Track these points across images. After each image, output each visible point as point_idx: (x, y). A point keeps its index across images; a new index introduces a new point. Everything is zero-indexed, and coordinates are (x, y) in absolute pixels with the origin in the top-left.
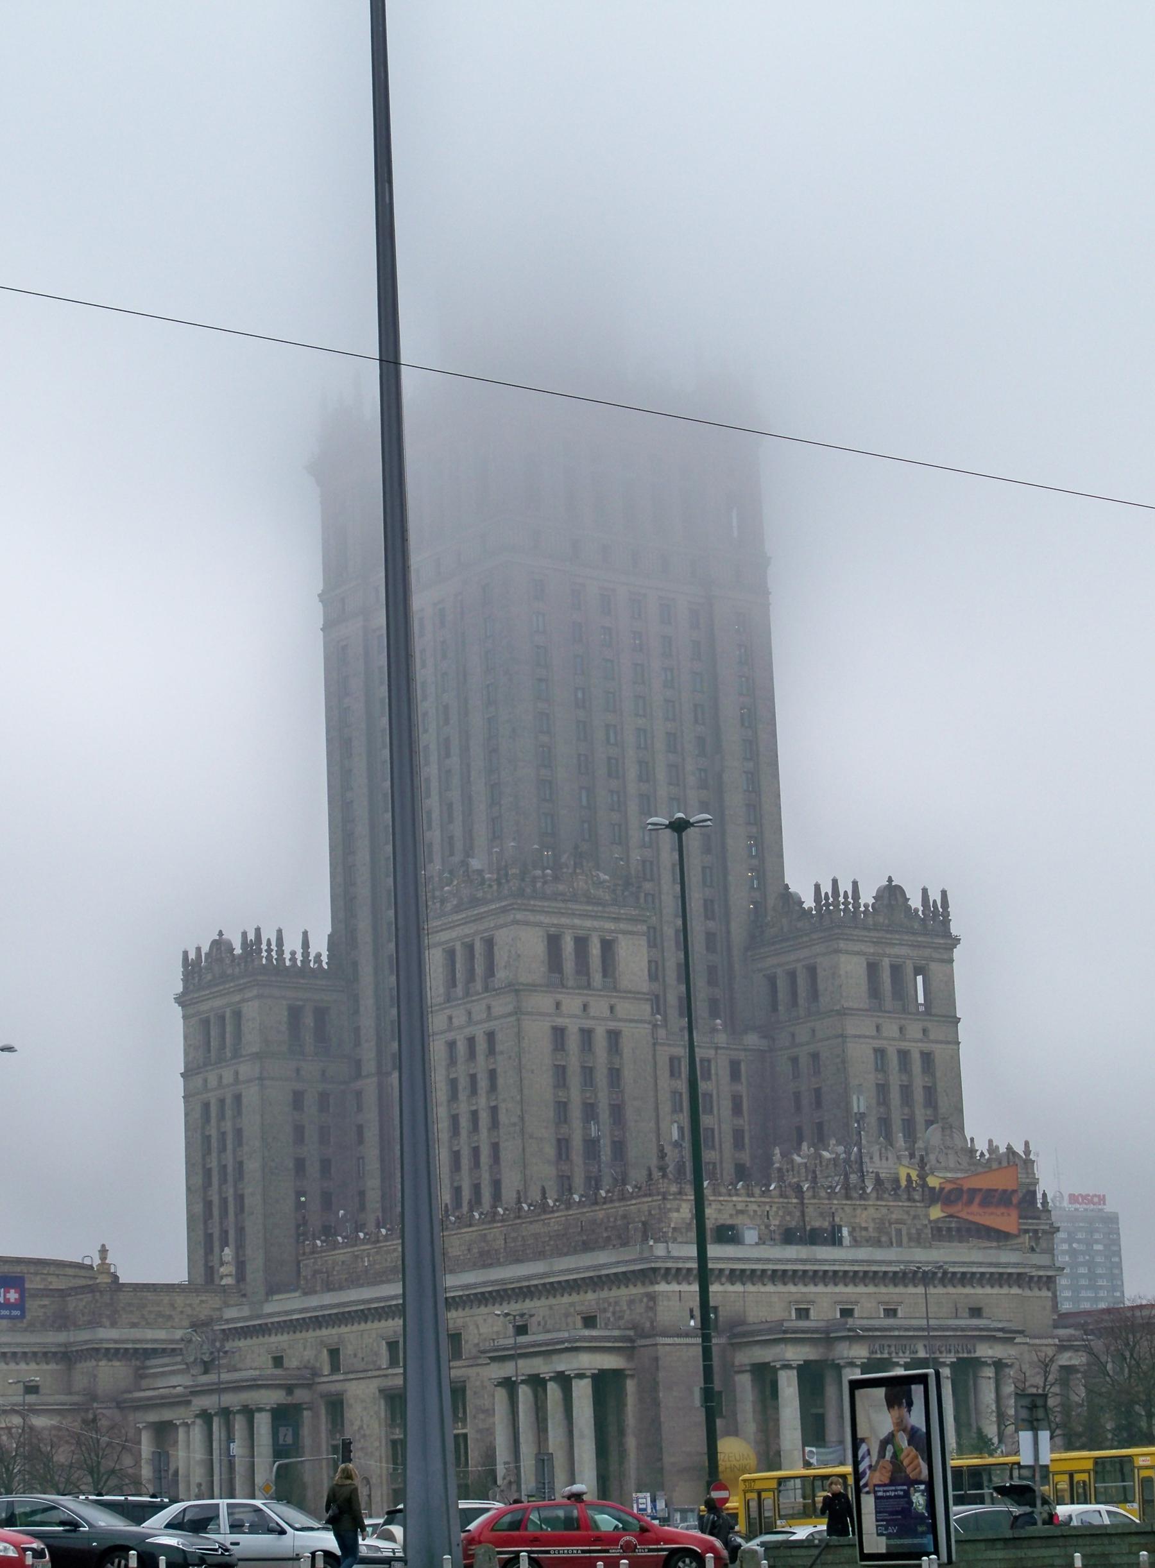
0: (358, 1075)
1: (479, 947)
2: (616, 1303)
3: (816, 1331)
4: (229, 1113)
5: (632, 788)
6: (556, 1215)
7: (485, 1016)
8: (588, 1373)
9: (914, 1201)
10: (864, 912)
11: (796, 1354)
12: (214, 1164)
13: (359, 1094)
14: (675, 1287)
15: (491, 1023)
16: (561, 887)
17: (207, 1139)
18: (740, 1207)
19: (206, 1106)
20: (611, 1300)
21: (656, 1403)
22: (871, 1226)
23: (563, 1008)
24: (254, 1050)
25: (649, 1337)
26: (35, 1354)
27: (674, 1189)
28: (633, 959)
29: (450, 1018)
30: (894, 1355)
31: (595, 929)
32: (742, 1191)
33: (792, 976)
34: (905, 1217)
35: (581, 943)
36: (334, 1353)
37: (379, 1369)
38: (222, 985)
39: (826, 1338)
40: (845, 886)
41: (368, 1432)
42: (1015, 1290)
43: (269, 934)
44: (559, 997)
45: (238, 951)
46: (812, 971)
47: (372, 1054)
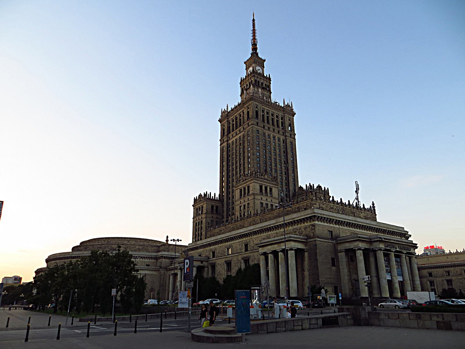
0: (223, 218)
1: (246, 188)
2: (300, 229)
3: (367, 238)
4: (200, 224)
5: (273, 167)
6: (276, 211)
7: (247, 200)
8: (294, 249)
9: (373, 213)
12: (197, 233)
14: (320, 223)
15: (249, 201)
16: (263, 177)
17: (196, 229)
18: (332, 206)
19: (196, 223)
20: (298, 228)
21: (316, 260)
23: (263, 199)
25: (312, 238)
26: (149, 257)
28: (275, 191)
29: (241, 202)
30: (391, 248)
31: (268, 185)
32: (332, 202)
34: (371, 217)
35: (266, 188)
36: (214, 253)
37: (225, 256)
38: (201, 203)
41: (221, 273)
43: (208, 193)
44: (262, 197)
45: (203, 196)
47: (226, 214)
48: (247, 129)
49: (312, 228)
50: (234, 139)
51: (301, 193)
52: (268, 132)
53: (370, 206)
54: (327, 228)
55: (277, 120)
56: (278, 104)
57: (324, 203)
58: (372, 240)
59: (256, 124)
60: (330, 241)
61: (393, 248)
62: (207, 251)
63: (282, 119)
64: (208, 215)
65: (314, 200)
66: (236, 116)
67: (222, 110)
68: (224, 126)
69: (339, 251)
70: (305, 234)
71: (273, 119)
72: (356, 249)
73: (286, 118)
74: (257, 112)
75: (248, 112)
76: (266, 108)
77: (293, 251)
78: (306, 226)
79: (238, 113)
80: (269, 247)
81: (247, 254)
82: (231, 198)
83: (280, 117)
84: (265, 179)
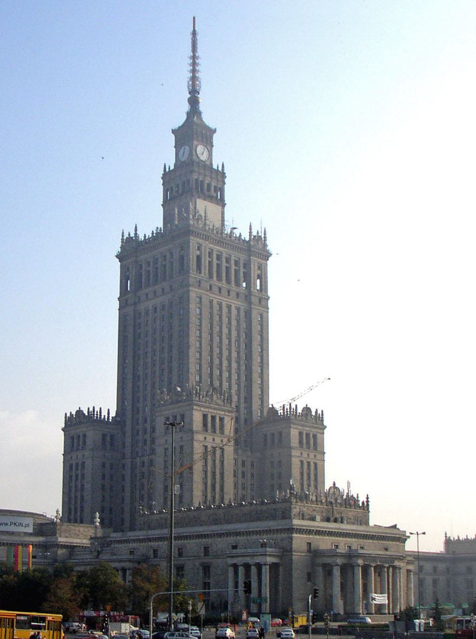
0: (124, 458)
4: (80, 468)
11: (340, 561)
13: (124, 465)
18: (314, 508)
19: (71, 466)
22: (352, 518)
24: (90, 447)
25: (289, 552)
29: (166, 441)
32: (315, 503)
33: (273, 435)
35: (213, 418)
42: (398, 543)
44: (206, 435)
46: (280, 434)
50: (149, 304)
55: (235, 270)
57: (306, 505)
63: (245, 266)
67: (123, 233)
68: (128, 269)
72: (334, 564)
74: (199, 258)
76: (214, 247)
80: (240, 559)
81: (207, 560)
82: (140, 421)
83: (242, 262)
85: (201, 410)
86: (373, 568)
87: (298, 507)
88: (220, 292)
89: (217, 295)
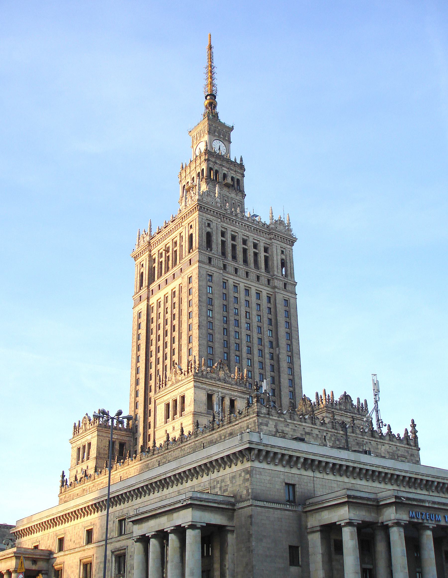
2: (223, 481)
3: (368, 499)
5: (244, 355)
6: (188, 442)
8: (199, 525)
9: (411, 445)
10: (336, 404)
14: (264, 465)
16: (214, 375)
18: (307, 430)
20: (219, 479)
27: (264, 410)
30: (425, 521)
32: (308, 421)
34: (406, 454)
36: (61, 541)
39: (377, 506)
40: (328, 393)
48: (188, 271)
49: (244, 477)
51: (306, 412)
52: (235, 278)
53: (406, 430)
54: (282, 477)
56: (257, 219)
58: (381, 503)
59: (207, 261)
60: (288, 506)
61: (432, 520)
62: (50, 536)
63: (266, 250)
64: (99, 461)
65: (262, 415)
66: (167, 246)
68: (142, 265)
69: (309, 530)
70: (233, 491)
71: (245, 251)
73: (274, 249)
74: (209, 235)
75: (191, 236)
76: (229, 226)
77: (197, 532)
78: (234, 474)
79: (170, 237)
84: (219, 380)
85: (204, 389)
86: (429, 533)
87: (272, 424)
88: (236, 273)
89: (232, 275)
